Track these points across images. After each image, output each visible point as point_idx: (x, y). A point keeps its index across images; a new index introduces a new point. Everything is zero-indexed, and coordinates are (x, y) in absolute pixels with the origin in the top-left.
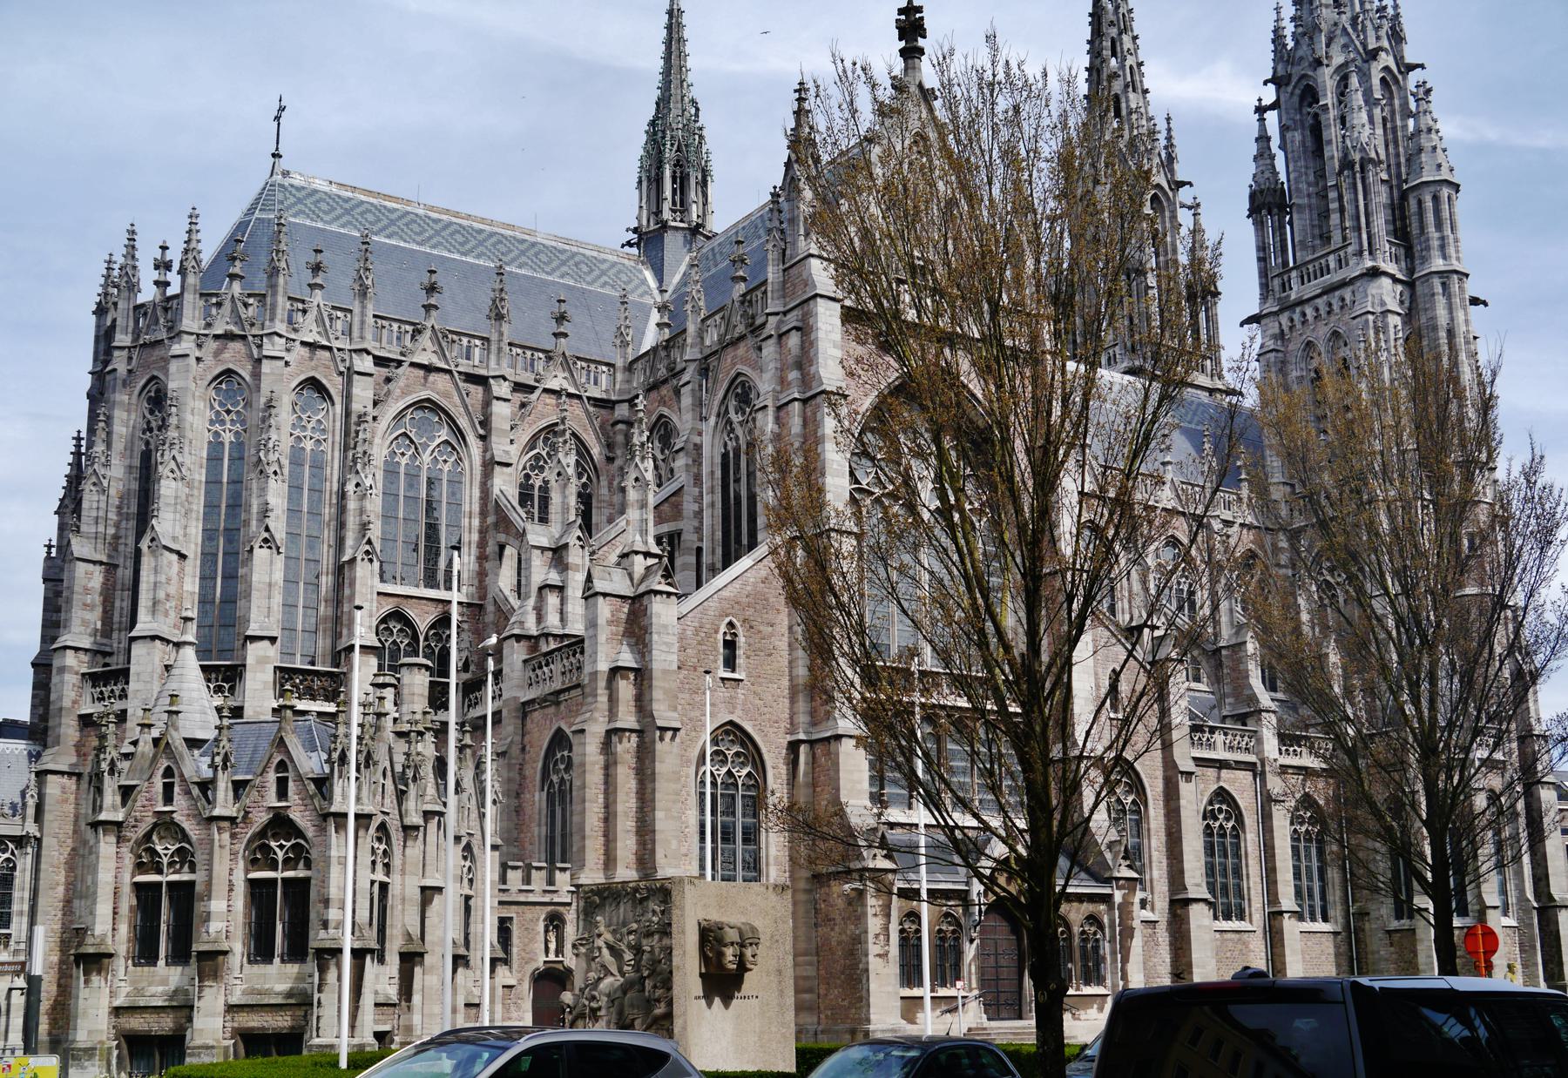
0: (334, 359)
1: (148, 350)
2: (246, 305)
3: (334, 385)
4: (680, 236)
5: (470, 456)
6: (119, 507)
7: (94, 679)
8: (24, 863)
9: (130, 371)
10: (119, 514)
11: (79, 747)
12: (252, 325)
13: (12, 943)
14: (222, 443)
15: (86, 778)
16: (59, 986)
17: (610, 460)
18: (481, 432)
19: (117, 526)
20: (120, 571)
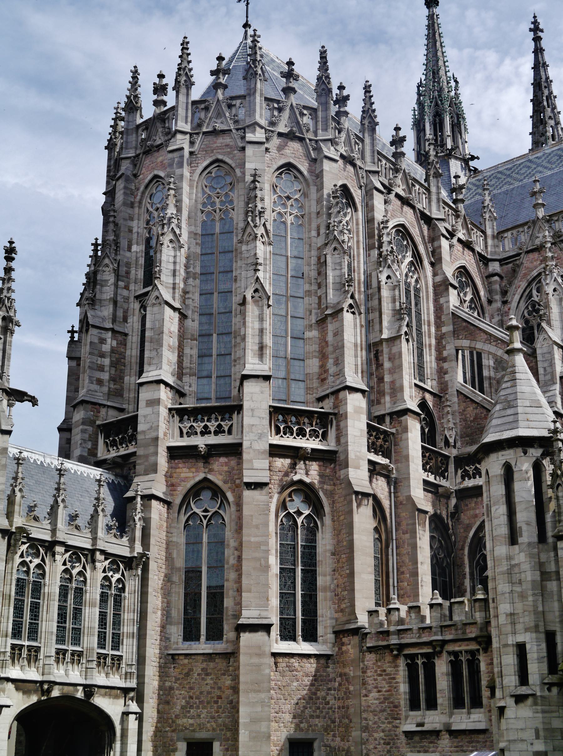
0: (357, 174)
1: (210, 138)
2: (302, 115)
3: (357, 194)
4: (459, 163)
5: (426, 277)
6: (187, 266)
7: (180, 413)
8: (132, 584)
9: (191, 153)
10: (187, 273)
11: (168, 476)
12: (308, 131)
13: (123, 665)
14: (284, 223)
15: (176, 508)
16: (158, 712)
17: (490, 302)
18: (432, 260)
19: (185, 280)
20: (188, 322)
